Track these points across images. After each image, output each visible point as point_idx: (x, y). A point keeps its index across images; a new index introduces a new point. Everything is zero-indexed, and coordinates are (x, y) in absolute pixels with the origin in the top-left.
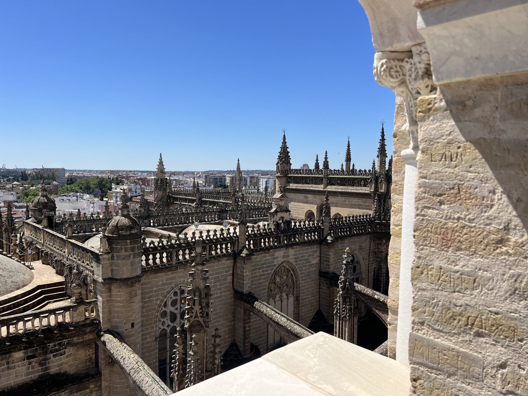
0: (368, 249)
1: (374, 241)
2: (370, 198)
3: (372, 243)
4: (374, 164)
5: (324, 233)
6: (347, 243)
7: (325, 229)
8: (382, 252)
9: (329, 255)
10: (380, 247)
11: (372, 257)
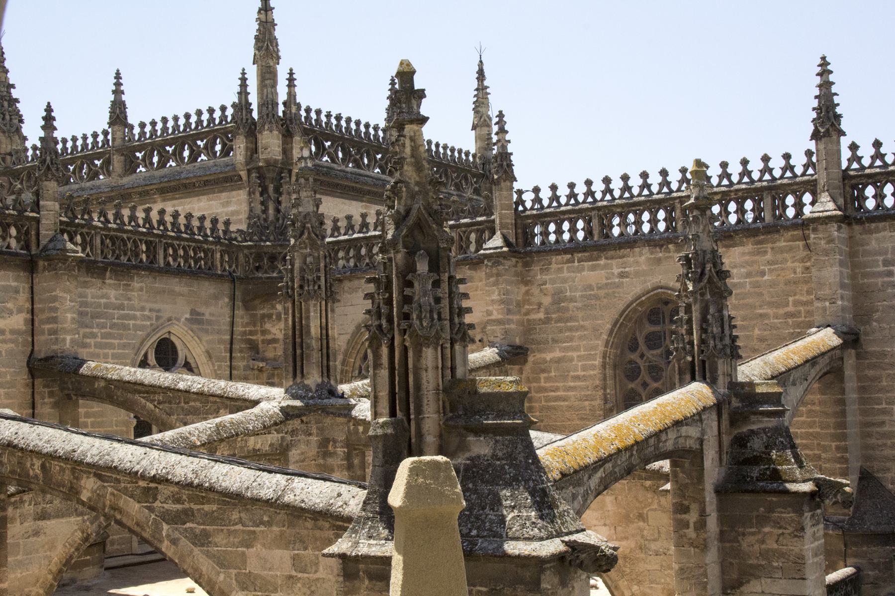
0: (228, 328)
1: (247, 306)
2: (240, 189)
3: (239, 312)
4: (243, 80)
5: (43, 232)
6: (141, 289)
7: (44, 221)
8: (275, 341)
9: (55, 299)
10: (268, 326)
11: (243, 358)
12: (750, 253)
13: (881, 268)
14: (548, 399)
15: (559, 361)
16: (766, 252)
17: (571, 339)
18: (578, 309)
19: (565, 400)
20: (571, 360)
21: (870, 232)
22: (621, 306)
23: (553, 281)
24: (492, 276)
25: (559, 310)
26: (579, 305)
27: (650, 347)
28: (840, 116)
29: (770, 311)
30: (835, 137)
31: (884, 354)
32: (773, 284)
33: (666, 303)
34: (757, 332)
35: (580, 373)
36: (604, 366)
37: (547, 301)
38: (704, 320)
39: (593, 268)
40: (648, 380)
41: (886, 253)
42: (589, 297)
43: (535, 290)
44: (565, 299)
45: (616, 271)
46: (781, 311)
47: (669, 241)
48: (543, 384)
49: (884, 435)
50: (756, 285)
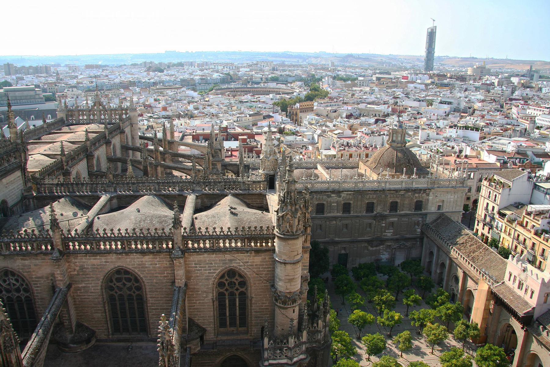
12: (151, 258)
13: (194, 265)
14: (81, 299)
15: (84, 287)
16: (157, 258)
17: (89, 281)
18: (90, 271)
19: (88, 299)
20: (89, 287)
21: (190, 255)
22: (106, 272)
23: (79, 262)
24: (56, 265)
25: (83, 271)
26: (91, 270)
27: (117, 282)
28: (181, 221)
29: (159, 275)
30: (180, 228)
31: (195, 288)
32: (159, 268)
33: (122, 269)
34: (155, 281)
35: (93, 291)
36: (102, 289)
37: (77, 268)
38: (169, 361)
39: (95, 259)
40: (117, 291)
41: (195, 261)
42: (94, 268)
43: (72, 265)
44: (85, 268)
45: (104, 261)
46: (162, 275)
47: (122, 253)
48: (79, 294)
49: (195, 309)
50: (154, 268)
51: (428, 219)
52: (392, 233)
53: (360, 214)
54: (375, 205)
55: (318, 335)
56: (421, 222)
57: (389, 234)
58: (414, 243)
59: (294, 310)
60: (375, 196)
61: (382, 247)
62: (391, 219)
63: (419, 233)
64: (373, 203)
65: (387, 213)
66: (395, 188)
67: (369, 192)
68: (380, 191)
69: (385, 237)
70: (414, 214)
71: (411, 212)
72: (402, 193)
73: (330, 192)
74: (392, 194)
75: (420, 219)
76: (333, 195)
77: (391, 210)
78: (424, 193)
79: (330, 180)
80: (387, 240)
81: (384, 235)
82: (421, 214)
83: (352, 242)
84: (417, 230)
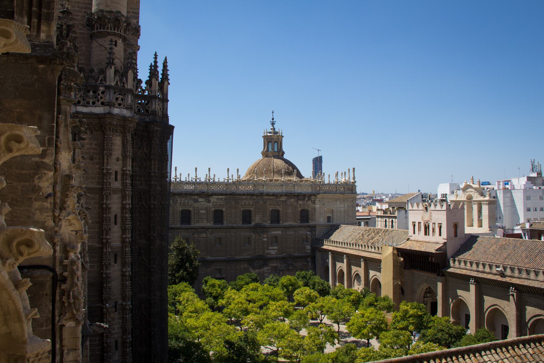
51: (317, 233)
52: (276, 251)
53: (235, 225)
54: (253, 213)
55: (152, 104)
56: (309, 236)
57: (273, 251)
58: (305, 263)
59: (116, 42)
60: (251, 203)
61: (266, 268)
62: (274, 232)
63: (309, 251)
64: (250, 211)
65: (268, 223)
66: (274, 192)
67: (244, 197)
68: (257, 195)
69: (269, 256)
70: (300, 227)
71: (296, 224)
72: (283, 198)
73: (197, 195)
74: (272, 199)
75: (308, 233)
76: (200, 200)
77: (272, 222)
78: (309, 200)
79: (196, 180)
80: (271, 259)
81: (268, 253)
82: (308, 226)
83: (229, 261)
84: (306, 246)
